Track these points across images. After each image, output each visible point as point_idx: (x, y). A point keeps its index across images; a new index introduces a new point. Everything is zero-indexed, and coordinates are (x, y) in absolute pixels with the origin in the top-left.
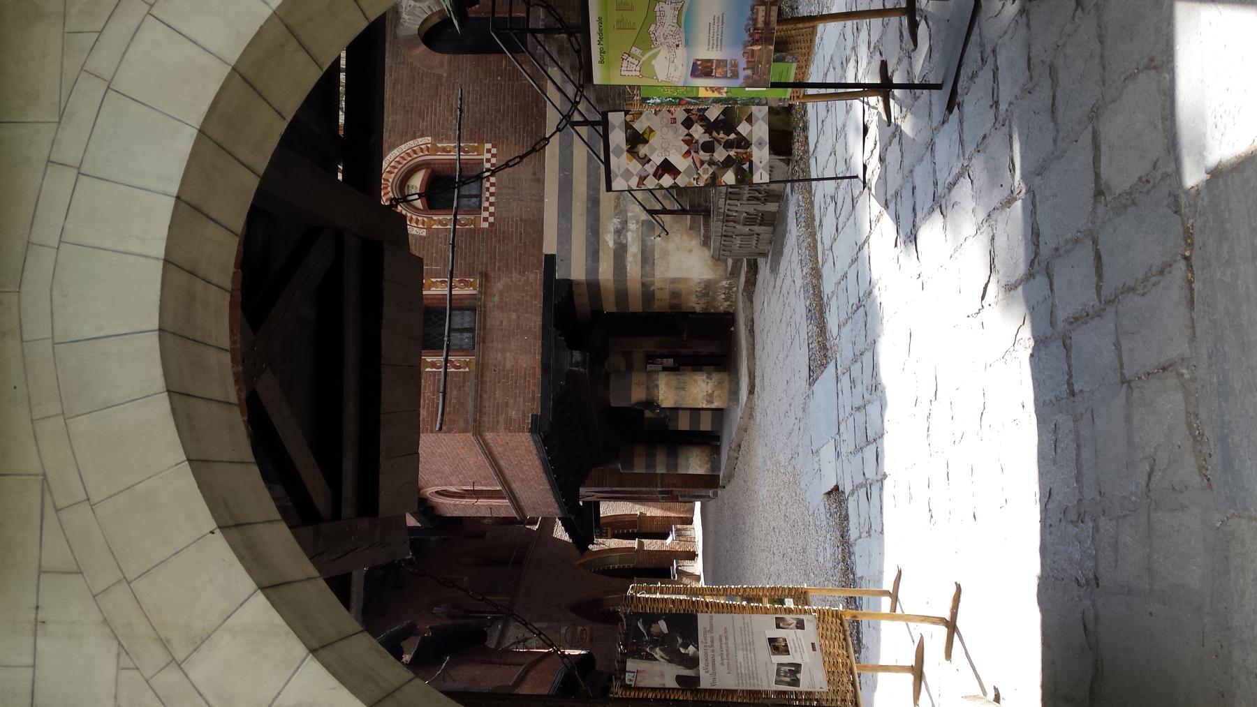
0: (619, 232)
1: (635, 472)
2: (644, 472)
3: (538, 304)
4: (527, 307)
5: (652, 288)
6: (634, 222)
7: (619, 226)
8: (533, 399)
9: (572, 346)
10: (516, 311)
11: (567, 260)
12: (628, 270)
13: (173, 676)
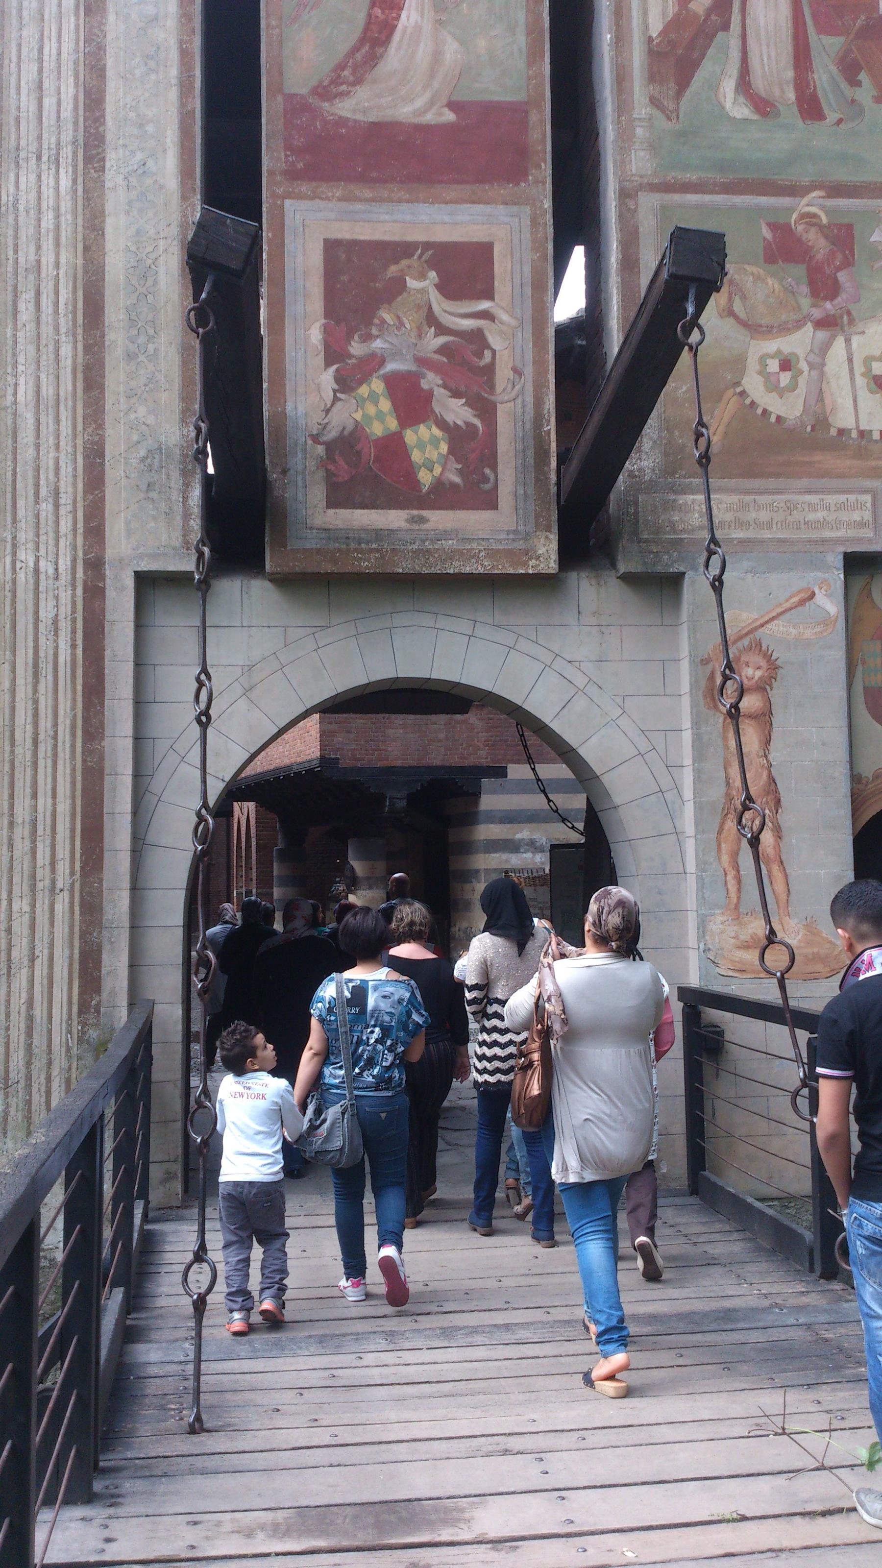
1: (275, 866)
2: (275, 874)
3: (455, 761)
4: (450, 749)
5: (473, 880)
7: (538, 844)
8: (356, 759)
9: (412, 799)
10: (447, 738)
12: (492, 855)
13: (239, 691)
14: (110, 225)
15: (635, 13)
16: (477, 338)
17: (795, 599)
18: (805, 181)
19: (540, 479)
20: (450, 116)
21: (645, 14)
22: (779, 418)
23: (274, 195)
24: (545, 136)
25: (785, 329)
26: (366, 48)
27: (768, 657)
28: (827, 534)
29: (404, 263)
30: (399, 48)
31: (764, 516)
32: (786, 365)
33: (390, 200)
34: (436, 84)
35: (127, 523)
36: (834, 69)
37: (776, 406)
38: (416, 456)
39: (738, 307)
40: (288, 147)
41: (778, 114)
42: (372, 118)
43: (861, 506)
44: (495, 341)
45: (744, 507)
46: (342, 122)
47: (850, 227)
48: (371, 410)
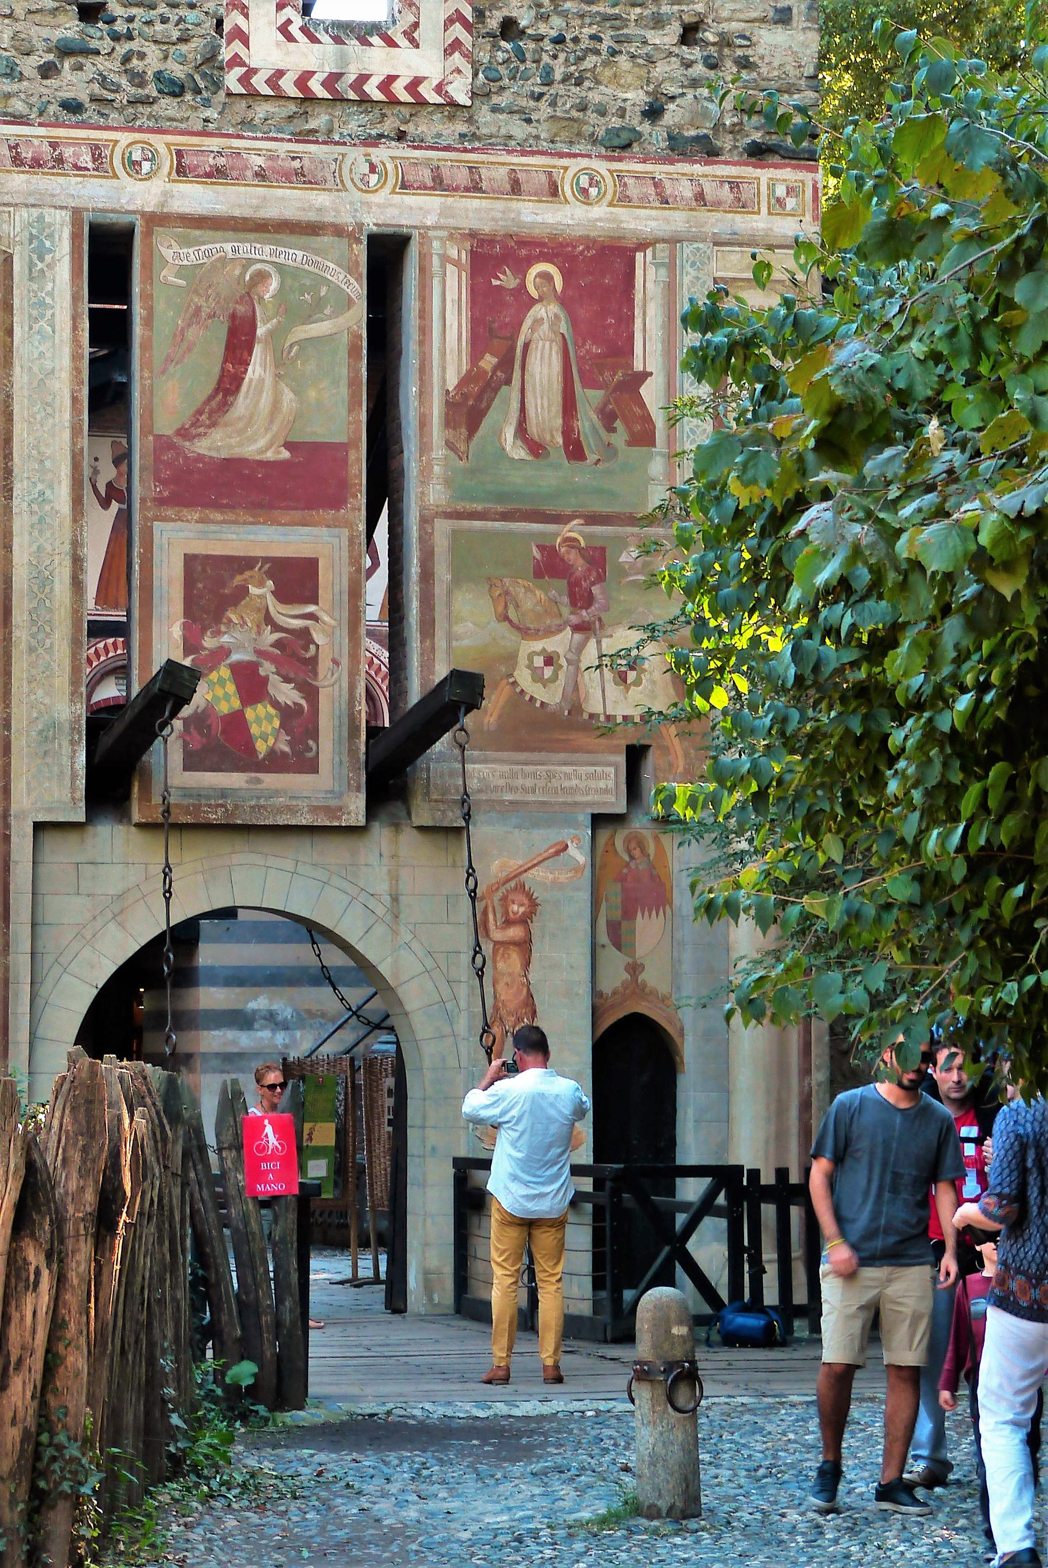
0: (271, 1018)
5: (182, 1068)
6: (287, 1041)
7: (280, 1018)
11: (229, 937)
13: (111, 916)
14: (16, 541)
15: (436, 371)
16: (305, 635)
17: (552, 851)
18: (568, 511)
19: (352, 752)
20: (285, 454)
21: (444, 369)
22: (542, 703)
23: (146, 519)
24: (360, 471)
25: (549, 632)
26: (220, 396)
27: (530, 896)
28: (579, 798)
29: (248, 574)
30: (246, 397)
31: (529, 783)
32: (549, 661)
33: (235, 522)
34: (275, 428)
35: (28, 783)
36: (594, 417)
37: (540, 694)
38: (254, 730)
39: (512, 614)
40: (158, 479)
41: (548, 454)
42: (224, 454)
43: (607, 776)
44: (318, 637)
45: (514, 775)
46: (200, 458)
47: (603, 549)
48: (220, 692)
